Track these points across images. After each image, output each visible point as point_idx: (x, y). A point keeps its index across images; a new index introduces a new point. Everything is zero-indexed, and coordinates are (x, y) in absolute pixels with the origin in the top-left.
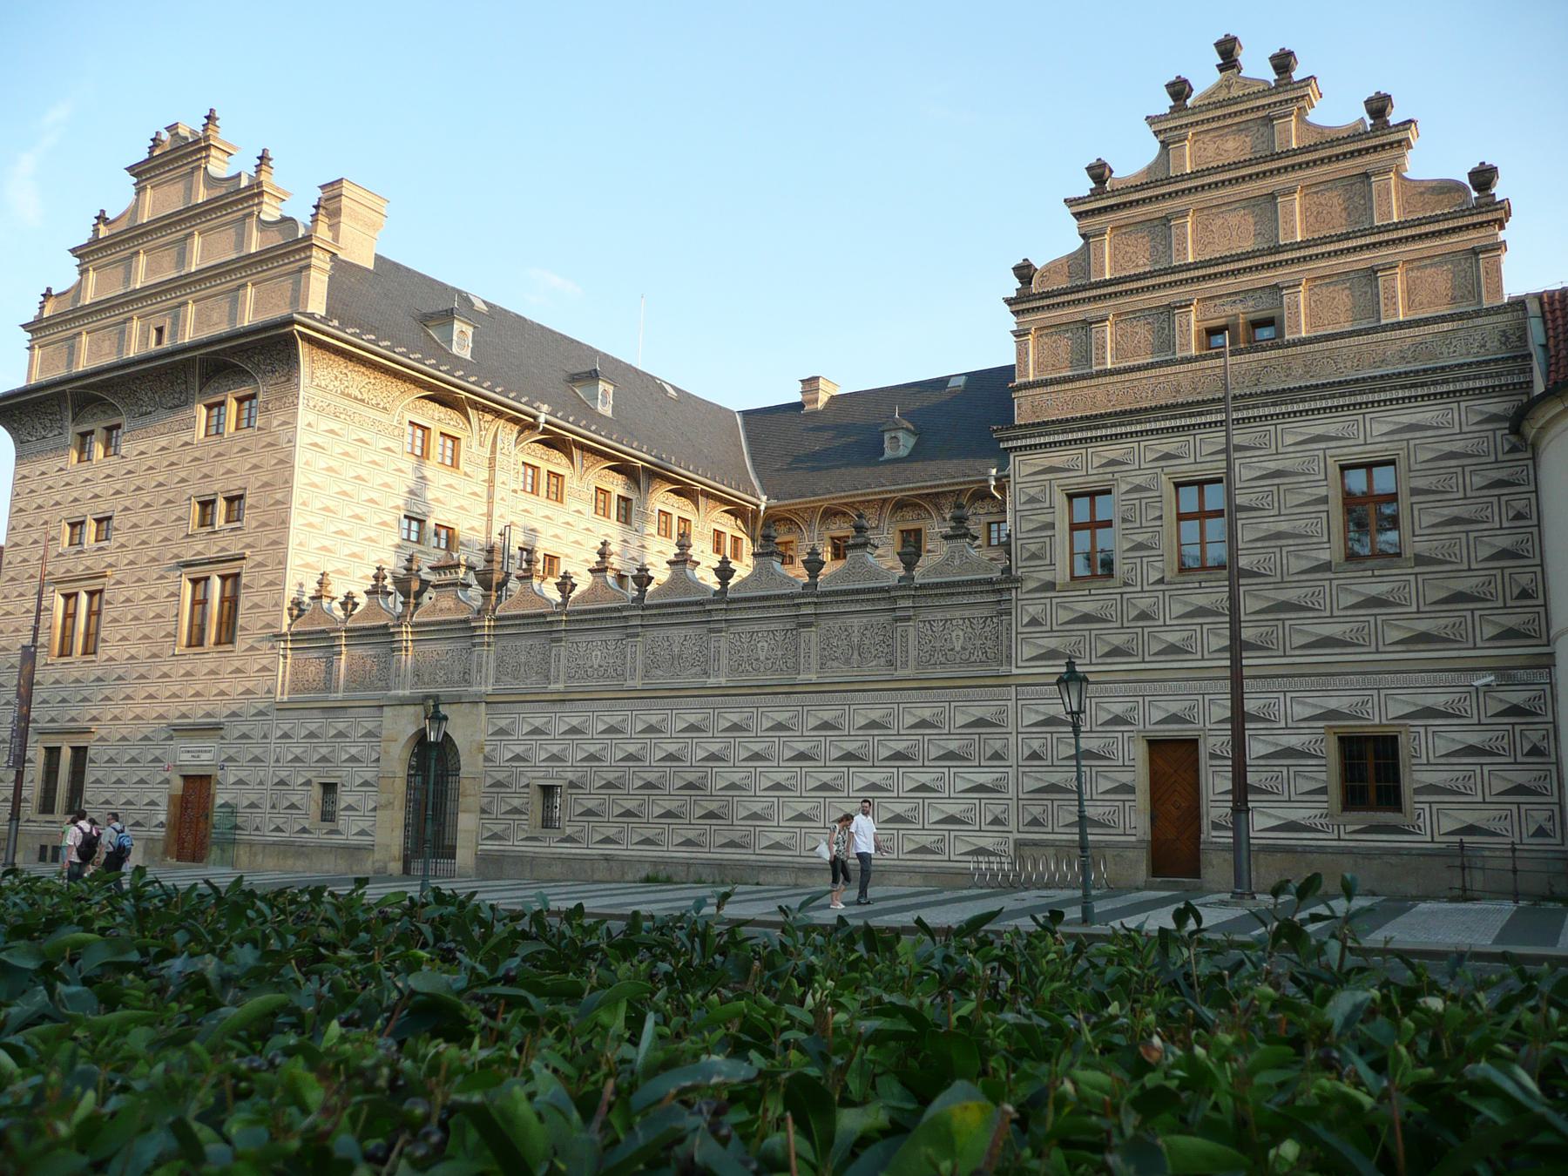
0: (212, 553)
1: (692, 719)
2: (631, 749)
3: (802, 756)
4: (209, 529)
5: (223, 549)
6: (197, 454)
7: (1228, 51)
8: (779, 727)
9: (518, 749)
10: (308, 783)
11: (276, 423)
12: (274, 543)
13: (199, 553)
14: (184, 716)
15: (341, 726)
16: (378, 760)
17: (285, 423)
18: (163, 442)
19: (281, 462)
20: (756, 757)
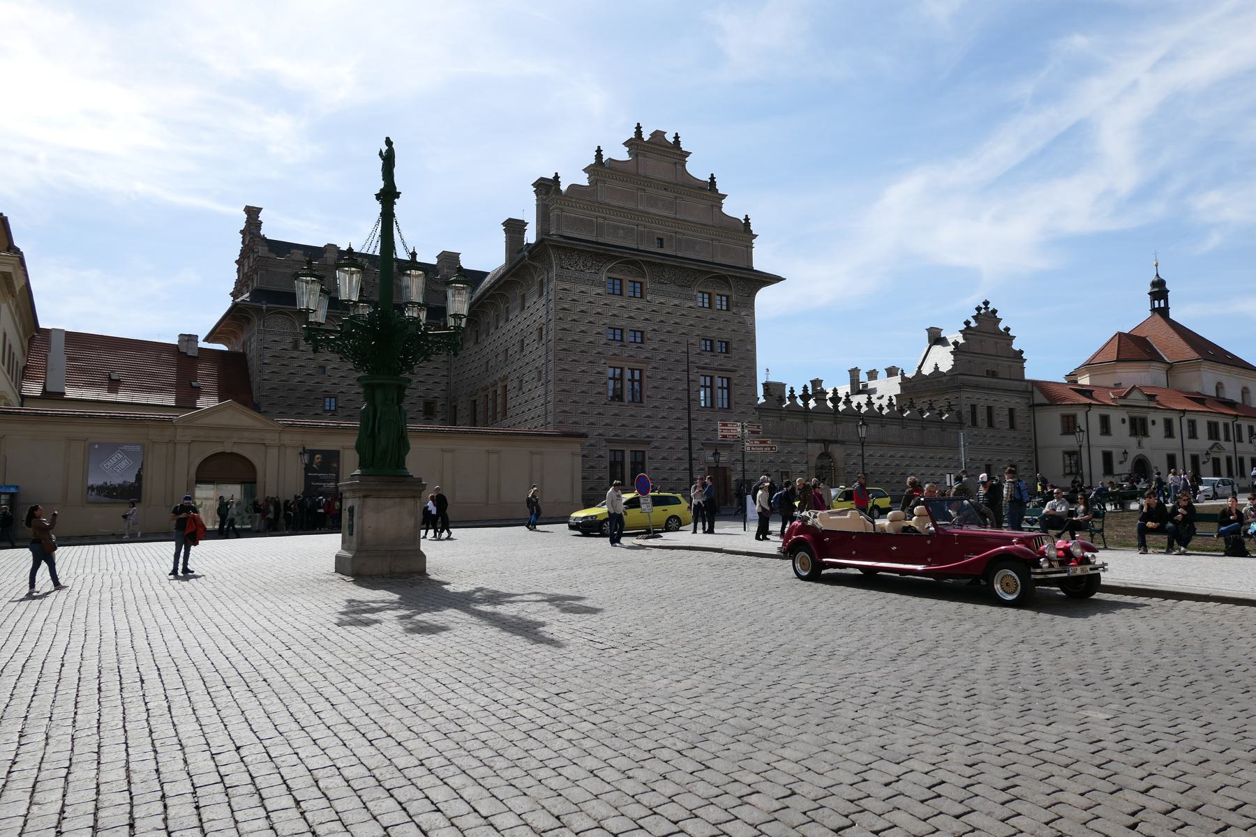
0: (715, 365)
1: (902, 454)
2: (887, 462)
3: (927, 466)
4: (712, 354)
5: (720, 365)
6: (699, 315)
7: (986, 303)
8: (922, 457)
9: (855, 461)
10: (777, 471)
11: (743, 314)
12: (748, 368)
13: (706, 364)
14: (708, 439)
15: (790, 449)
16: (807, 463)
17: (747, 315)
18: (677, 303)
19: (747, 332)
20: (918, 466)
